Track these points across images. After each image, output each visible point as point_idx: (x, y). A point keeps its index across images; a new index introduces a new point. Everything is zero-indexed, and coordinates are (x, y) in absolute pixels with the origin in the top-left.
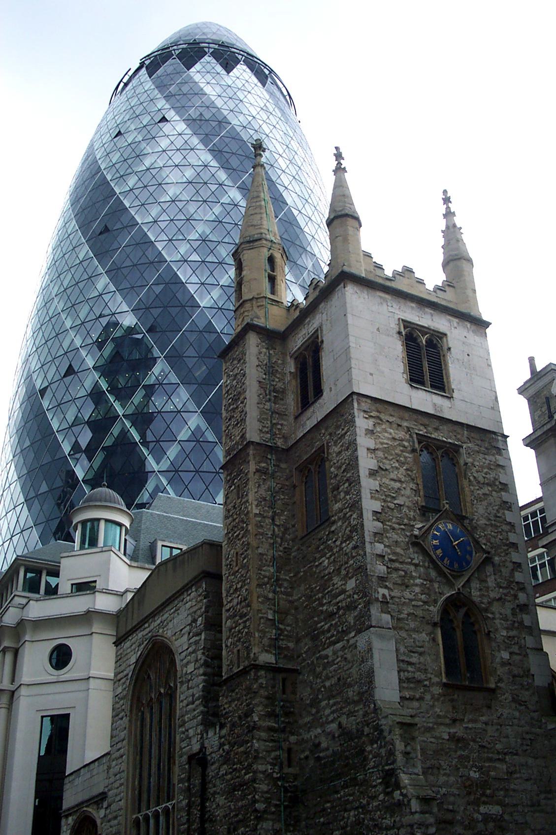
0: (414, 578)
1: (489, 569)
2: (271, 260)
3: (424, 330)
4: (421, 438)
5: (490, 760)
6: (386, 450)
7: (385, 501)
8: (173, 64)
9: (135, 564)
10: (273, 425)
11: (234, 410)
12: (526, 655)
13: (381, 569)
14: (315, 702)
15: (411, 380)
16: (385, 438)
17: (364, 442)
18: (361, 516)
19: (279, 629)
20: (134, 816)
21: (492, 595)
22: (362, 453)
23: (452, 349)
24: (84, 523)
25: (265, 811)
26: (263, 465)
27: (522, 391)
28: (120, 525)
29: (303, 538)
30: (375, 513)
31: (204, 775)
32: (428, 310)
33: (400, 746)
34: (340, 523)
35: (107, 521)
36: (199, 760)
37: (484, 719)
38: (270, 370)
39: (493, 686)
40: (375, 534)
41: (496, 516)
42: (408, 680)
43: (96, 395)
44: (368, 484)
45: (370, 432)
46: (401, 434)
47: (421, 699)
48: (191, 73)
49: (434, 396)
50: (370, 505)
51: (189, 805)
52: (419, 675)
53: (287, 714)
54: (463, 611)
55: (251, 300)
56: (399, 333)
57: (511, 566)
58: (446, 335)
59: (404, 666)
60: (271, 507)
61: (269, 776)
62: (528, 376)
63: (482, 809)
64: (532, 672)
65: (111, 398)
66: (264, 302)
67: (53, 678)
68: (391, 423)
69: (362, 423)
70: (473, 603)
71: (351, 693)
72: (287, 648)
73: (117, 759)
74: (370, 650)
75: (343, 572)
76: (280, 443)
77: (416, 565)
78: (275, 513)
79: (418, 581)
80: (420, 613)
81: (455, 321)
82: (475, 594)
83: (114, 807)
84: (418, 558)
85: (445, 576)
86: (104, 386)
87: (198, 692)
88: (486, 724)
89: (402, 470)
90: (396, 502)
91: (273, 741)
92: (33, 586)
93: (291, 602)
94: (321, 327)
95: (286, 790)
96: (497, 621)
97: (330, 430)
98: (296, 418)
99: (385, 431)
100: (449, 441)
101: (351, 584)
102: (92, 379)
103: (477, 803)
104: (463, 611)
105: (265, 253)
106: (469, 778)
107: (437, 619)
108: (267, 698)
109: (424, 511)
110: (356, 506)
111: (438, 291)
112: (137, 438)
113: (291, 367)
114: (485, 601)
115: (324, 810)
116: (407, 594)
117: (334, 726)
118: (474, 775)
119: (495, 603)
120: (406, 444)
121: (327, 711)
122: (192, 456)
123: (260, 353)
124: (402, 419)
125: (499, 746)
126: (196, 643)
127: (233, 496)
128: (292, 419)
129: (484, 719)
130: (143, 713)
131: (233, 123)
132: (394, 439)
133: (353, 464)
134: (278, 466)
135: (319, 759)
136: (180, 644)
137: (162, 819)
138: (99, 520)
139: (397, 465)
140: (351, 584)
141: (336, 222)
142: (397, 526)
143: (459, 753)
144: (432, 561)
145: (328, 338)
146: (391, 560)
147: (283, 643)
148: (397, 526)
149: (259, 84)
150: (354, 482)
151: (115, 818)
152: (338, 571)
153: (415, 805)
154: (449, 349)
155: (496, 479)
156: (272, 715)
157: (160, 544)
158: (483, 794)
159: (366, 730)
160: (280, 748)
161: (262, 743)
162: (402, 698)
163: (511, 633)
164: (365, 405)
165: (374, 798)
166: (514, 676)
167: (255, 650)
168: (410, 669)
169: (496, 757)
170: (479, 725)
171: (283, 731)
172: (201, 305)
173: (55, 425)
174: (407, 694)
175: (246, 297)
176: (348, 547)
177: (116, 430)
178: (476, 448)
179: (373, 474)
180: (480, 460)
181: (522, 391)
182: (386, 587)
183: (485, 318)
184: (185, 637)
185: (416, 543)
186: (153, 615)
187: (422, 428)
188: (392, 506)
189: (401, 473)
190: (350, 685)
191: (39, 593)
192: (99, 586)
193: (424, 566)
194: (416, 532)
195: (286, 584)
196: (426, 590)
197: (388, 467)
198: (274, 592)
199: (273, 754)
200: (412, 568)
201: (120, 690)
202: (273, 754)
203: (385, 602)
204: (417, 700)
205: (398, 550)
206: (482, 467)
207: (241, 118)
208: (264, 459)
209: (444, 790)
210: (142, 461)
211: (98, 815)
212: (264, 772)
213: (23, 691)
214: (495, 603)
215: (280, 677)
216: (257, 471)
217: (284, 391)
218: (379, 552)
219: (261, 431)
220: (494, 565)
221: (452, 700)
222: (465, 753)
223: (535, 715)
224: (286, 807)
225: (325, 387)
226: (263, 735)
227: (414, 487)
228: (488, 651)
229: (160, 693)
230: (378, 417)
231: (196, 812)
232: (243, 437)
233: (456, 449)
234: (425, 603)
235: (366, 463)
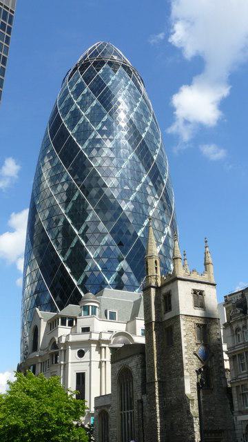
1: (213, 358)
2: (156, 262)
14: (171, 391)
16: (188, 325)
17: (182, 328)
22: (182, 331)
36: (141, 402)
46: (192, 324)
50: (184, 345)
67: (77, 361)
69: (182, 322)
71: (179, 390)
86: (70, 221)
92: (63, 323)
94: (170, 291)
101: (179, 364)
105: (154, 260)
110: (181, 345)
112: (84, 244)
113: (162, 298)
133: (179, 333)
136: (134, 370)
138: (89, 306)
140: (179, 364)
145: (172, 293)
150: (180, 338)
177: (75, 241)
179: (185, 336)
186: (124, 359)
210: (86, 253)
213: (70, 364)
235: (183, 333)
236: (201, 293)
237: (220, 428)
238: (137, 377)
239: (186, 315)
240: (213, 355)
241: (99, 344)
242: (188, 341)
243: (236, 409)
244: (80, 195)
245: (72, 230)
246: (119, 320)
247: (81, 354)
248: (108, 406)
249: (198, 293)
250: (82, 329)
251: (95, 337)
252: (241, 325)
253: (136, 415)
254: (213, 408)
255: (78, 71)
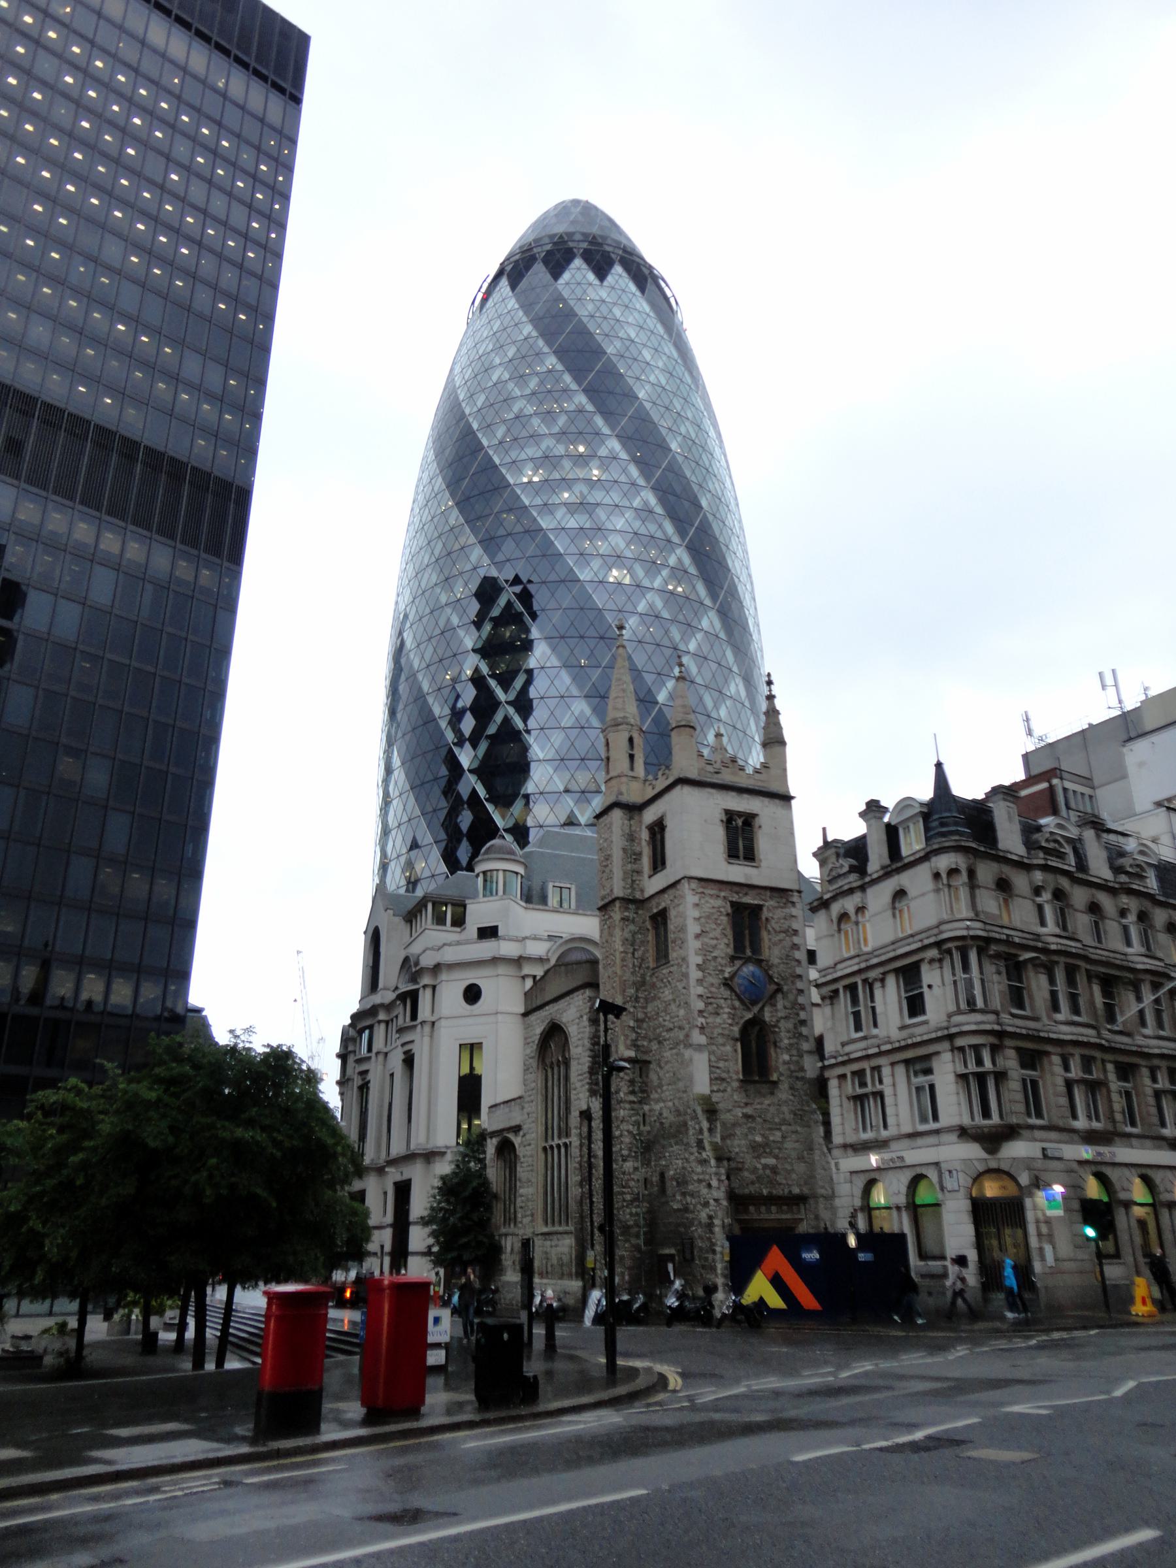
0: (722, 1008)
1: (779, 996)
2: (631, 740)
3: (740, 814)
4: (733, 904)
5: (771, 1129)
6: (708, 917)
7: (705, 955)
8: (539, 272)
9: (531, 906)
10: (633, 881)
11: (606, 866)
12: (801, 1056)
13: (700, 1005)
14: (660, 1086)
15: (729, 856)
16: (707, 908)
18: (688, 967)
19: (637, 1033)
20: (544, 1144)
21: (780, 1014)
23: (763, 827)
24: (484, 873)
25: (629, 1156)
26: (626, 914)
27: (815, 855)
28: (517, 873)
29: (653, 969)
30: (698, 965)
31: (590, 1127)
32: (745, 796)
33: (705, 1125)
34: (676, 967)
35: (504, 871)
36: (586, 1115)
37: (767, 1102)
38: (631, 838)
39: (774, 1077)
40: (698, 980)
41: (788, 956)
42: (716, 1079)
43: (478, 680)
44: (693, 945)
45: (697, 905)
46: (719, 902)
47: (724, 1091)
48: (560, 288)
49: (746, 868)
51: (581, 1145)
52: (724, 1075)
53: (643, 1091)
54: (757, 1028)
55: (616, 777)
56: (722, 821)
57: (795, 992)
58: (756, 815)
59: (713, 1069)
60: (632, 945)
61: (629, 1132)
62: (821, 844)
63: (763, 1161)
64: (806, 1068)
65: (493, 683)
66: (624, 779)
67: (467, 1013)
68: (712, 895)
70: (764, 1022)
71: (681, 1085)
72: (643, 1046)
73: (528, 1102)
74: (691, 1060)
75: (677, 1003)
76: (638, 896)
77: (725, 999)
78: (634, 950)
79: (727, 1010)
80: (726, 1032)
81: (766, 800)
82: (767, 1016)
83: (528, 1137)
84: (727, 993)
85: (746, 1005)
86: (485, 669)
87: (585, 1068)
88: (769, 1105)
89: (719, 930)
90: (714, 954)
91: (633, 1110)
92: (440, 920)
93: (646, 1013)
95: (642, 1142)
96: (782, 1034)
97: (672, 898)
98: (650, 877)
99: (707, 902)
100: (756, 902)
101: (682, 1012)
102: (471, 664)
103: (758, 1157)
104: (757, 1028)
105: (626, 736)
106: (755, 1142)
107: (737, 1035)
108: (629, 1081)
109: (733, 959)
110: (684, 959)
111: (757, 775)
113: (645, 835)
114: (774, 1020)
115: (665, 1157)
116: (718, 1020)
117: (670, 1104)
118: (759, 1139)
119: (782, 1021)
120: (722, 910)
121: (667, 1093)
122: (577, 744)
123: (623, 824)
124: (720, 890)
125: (777, 1120)
126: (583, 1032)
127: (606, 932)
128: (646, 876)
129: (767, 1102)
130: (547, 1071)
131: (608, 351)
132: (713, 907)
133: (682, 929)
134: (636, 913)
135: (662, 1124)
137: (563, 1150)
138: (497, 870)
139: (714, 926)
140: (682, 1012)
141: (675, 730)
142: (712, 972)
143: (749, 1125)
144: (737, 995)
145: (670, 824)
146: (708, 998)
147: (639, 1043)
148: (712, 972)
149: (638, 293)
151: (529, 1145)
152: (674, 1000)
153: (713, 1162)
154: (760, 827)
155: (789, 927)
156: (633, 1092)
157: (550, 885)
158: (765, 1152)
159: (689, 1111)
160: (638, 1114)
161: (626, 1112)
162: (712, 1091)
163: (792, 1041)
164: (694, 885)
165: (692, 1154)
166: (792, 1072)
167: (622, 1048)
168: (718, 1071)
169: (774, 1126)
170: (764, 1106)
171: (640, 1102)
172: (582, 578)
173: (437, 710)
174: (715, 1088)
175: (612, 774)
176: (680, 986)
177: (499, 718)
178: (776, 905)
179: (697, 936)
180: (779, 913)
181: (815, 855)
182: (704, 1017)
183: (792, 794)
184: (575, 1027)
185: (727, 983)
187: (735, 895)
188: (709, 958)
189: (717, 933)
190: (679, 1080)
191: (445, 924)
192: (500, 933)
193: (732, 999)
194: (727, 975)
195: (642, 1000)
196: (732, 1016)
197: (708, 929)
198: (634, 1007)
199: (633, 1119)
200: (722, 1001)
201: (528, 1051)
202: (633, 1119)
203: (702, 1028)
204: (722, 1092)
205: (713, 990)
206: (779, 919)
207: (618, 344)
208: (627, 909)
209: (737, 1150)
211: (517, 1140)
212: (628, 1131)
213: (443, 1023)
214: (782, 1021)
215: (637, 1066)
216: (623, 919)
217: (640, 854)
218: (699, 993)
219: (624, 888)
220: (783, 993)
221: (746, 1091)
222: (753, 1125)
223: (804, 1098)
224: (642, 1153)
225: (668, 862)
226: (627, 1106)
227: (726, 941)
228: (773, 1054)
229: (559, 1061)
230: (703, 893)
231: (585, 1150)
232: (612, 890)
233: (760, 907)
234: (731, 1025)
235: (693, 928)
236: (749, 819)
237: (796, 1190)
238: (580, 1050)
239: (701, 880)
240: (779, 990)
241: (519, 961)
242: (704, 951)
243: (837, 1139)
244: (509, 604)
245: (490, 693)
246: (578, 907)
247: (472, 994)
248: (517, 1129)
249: (740, 822)
250: (480, 930)
251: (507, 949)
252: (851, 910)
253: (575, 1151)
254: (777, 1136)
255: (504, 282)
